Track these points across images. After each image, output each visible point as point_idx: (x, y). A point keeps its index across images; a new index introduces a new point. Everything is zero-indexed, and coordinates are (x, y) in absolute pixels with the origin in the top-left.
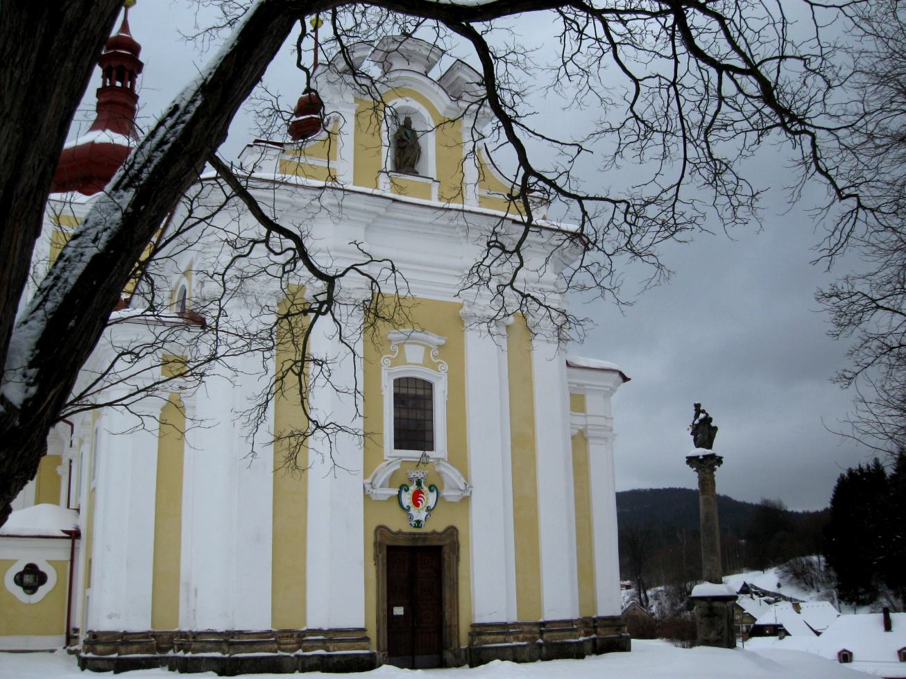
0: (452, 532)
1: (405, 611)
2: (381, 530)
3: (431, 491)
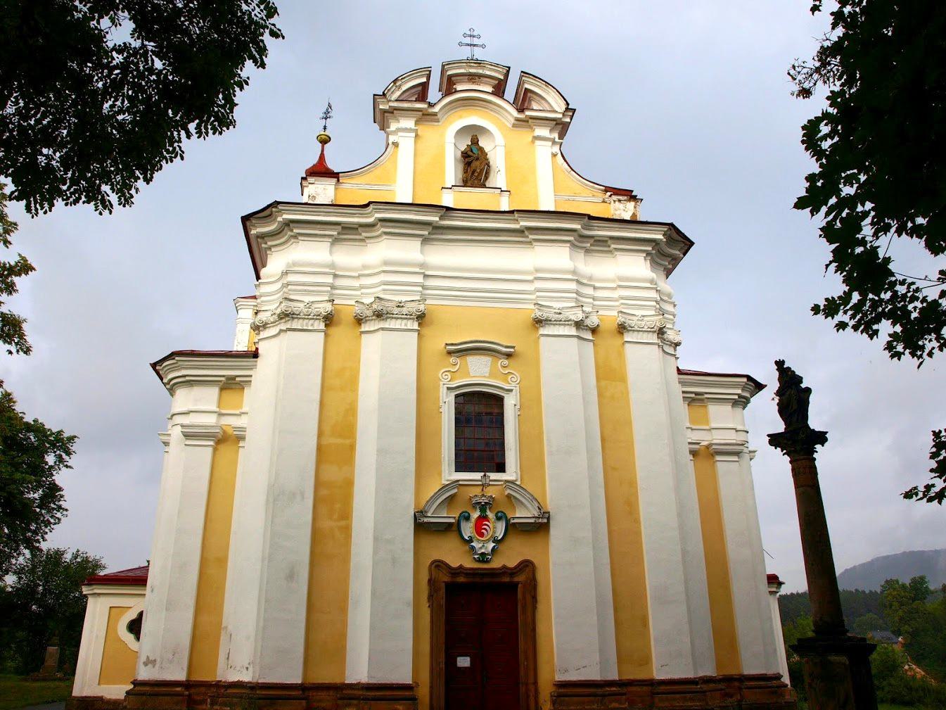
0: (527, 566)
1: (471, 661)
2: (438, 565)
3: (499, 519)
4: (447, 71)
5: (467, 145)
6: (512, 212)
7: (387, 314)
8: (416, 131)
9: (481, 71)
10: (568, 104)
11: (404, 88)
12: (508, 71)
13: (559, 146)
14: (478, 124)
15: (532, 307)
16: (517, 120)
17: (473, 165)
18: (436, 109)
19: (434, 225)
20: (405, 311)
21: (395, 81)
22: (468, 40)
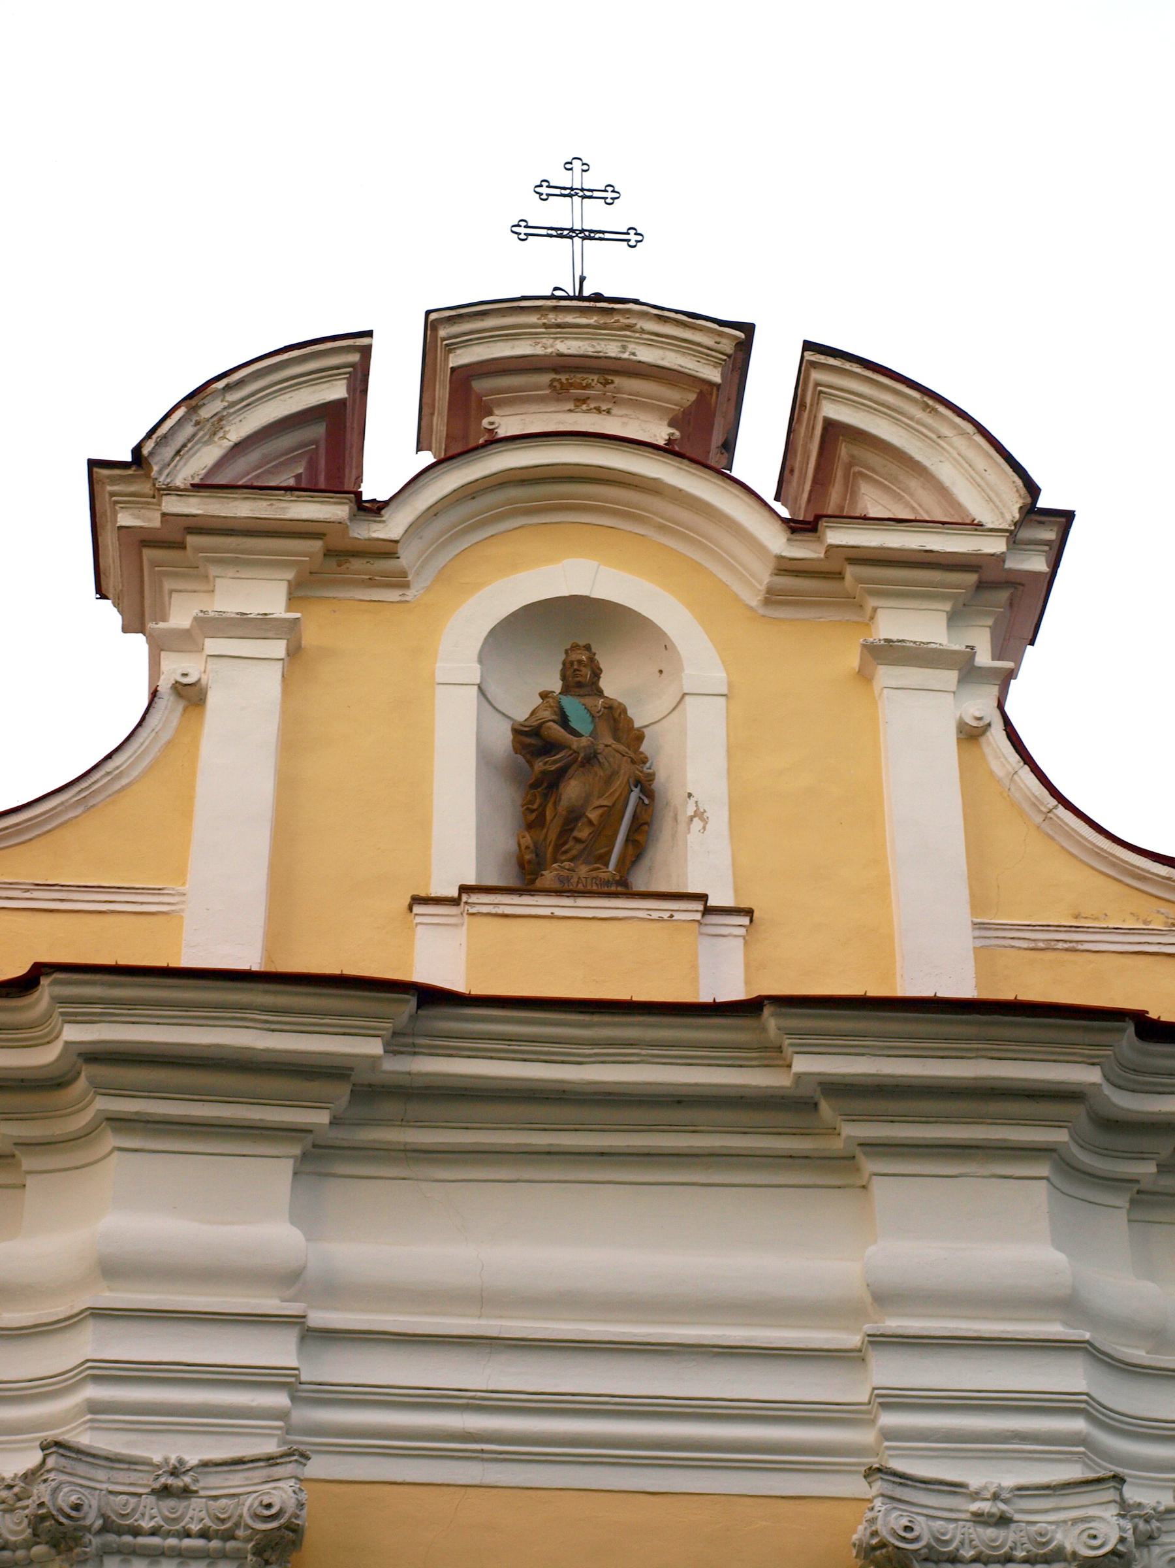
4: (450, 349)
5: (544, 695)
6: (751, 1007)
7: (104, 1529)
8: (289, 630)
9: (611, 349)
10: (1032, 489)
11: (237, 431)
12: (744, 347)
13: (995, 691)
14: (598, 593)
15: (855, 1486)
16: (786, 568)
17: (572, 790)
18: (392, 527)
20: (195, 1514)
21: (195, 398)
22: (559, 213)
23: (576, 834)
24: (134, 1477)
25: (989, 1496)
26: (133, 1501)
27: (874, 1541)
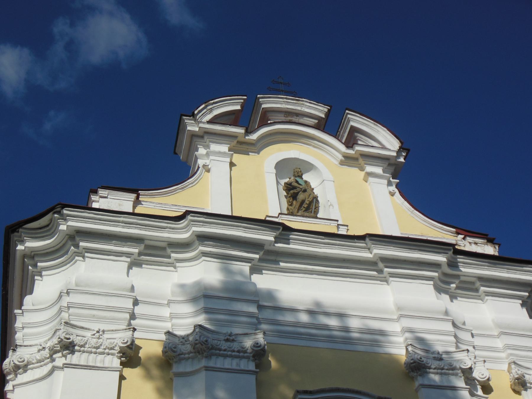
17: (301, 197)
19: (266, 247)
23: (303, 206)
24: (218, 337)
25: (436, 353)
26: (219, 342)
27: (412, 361)
